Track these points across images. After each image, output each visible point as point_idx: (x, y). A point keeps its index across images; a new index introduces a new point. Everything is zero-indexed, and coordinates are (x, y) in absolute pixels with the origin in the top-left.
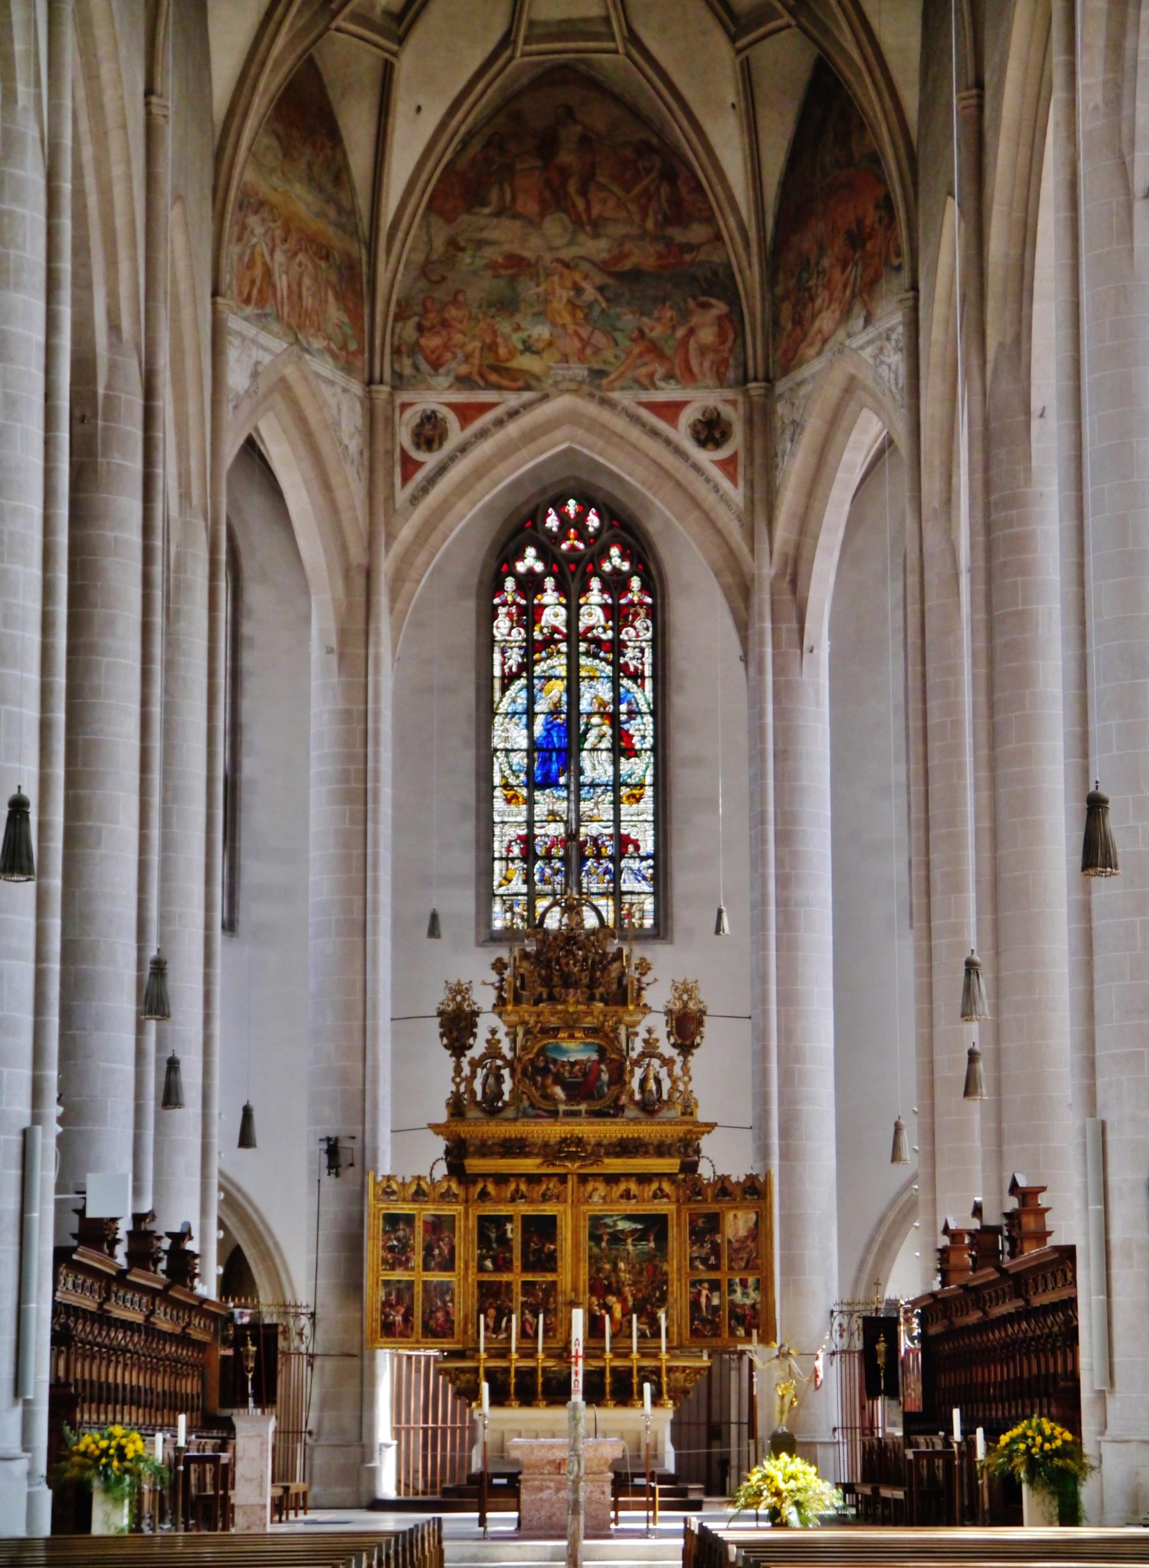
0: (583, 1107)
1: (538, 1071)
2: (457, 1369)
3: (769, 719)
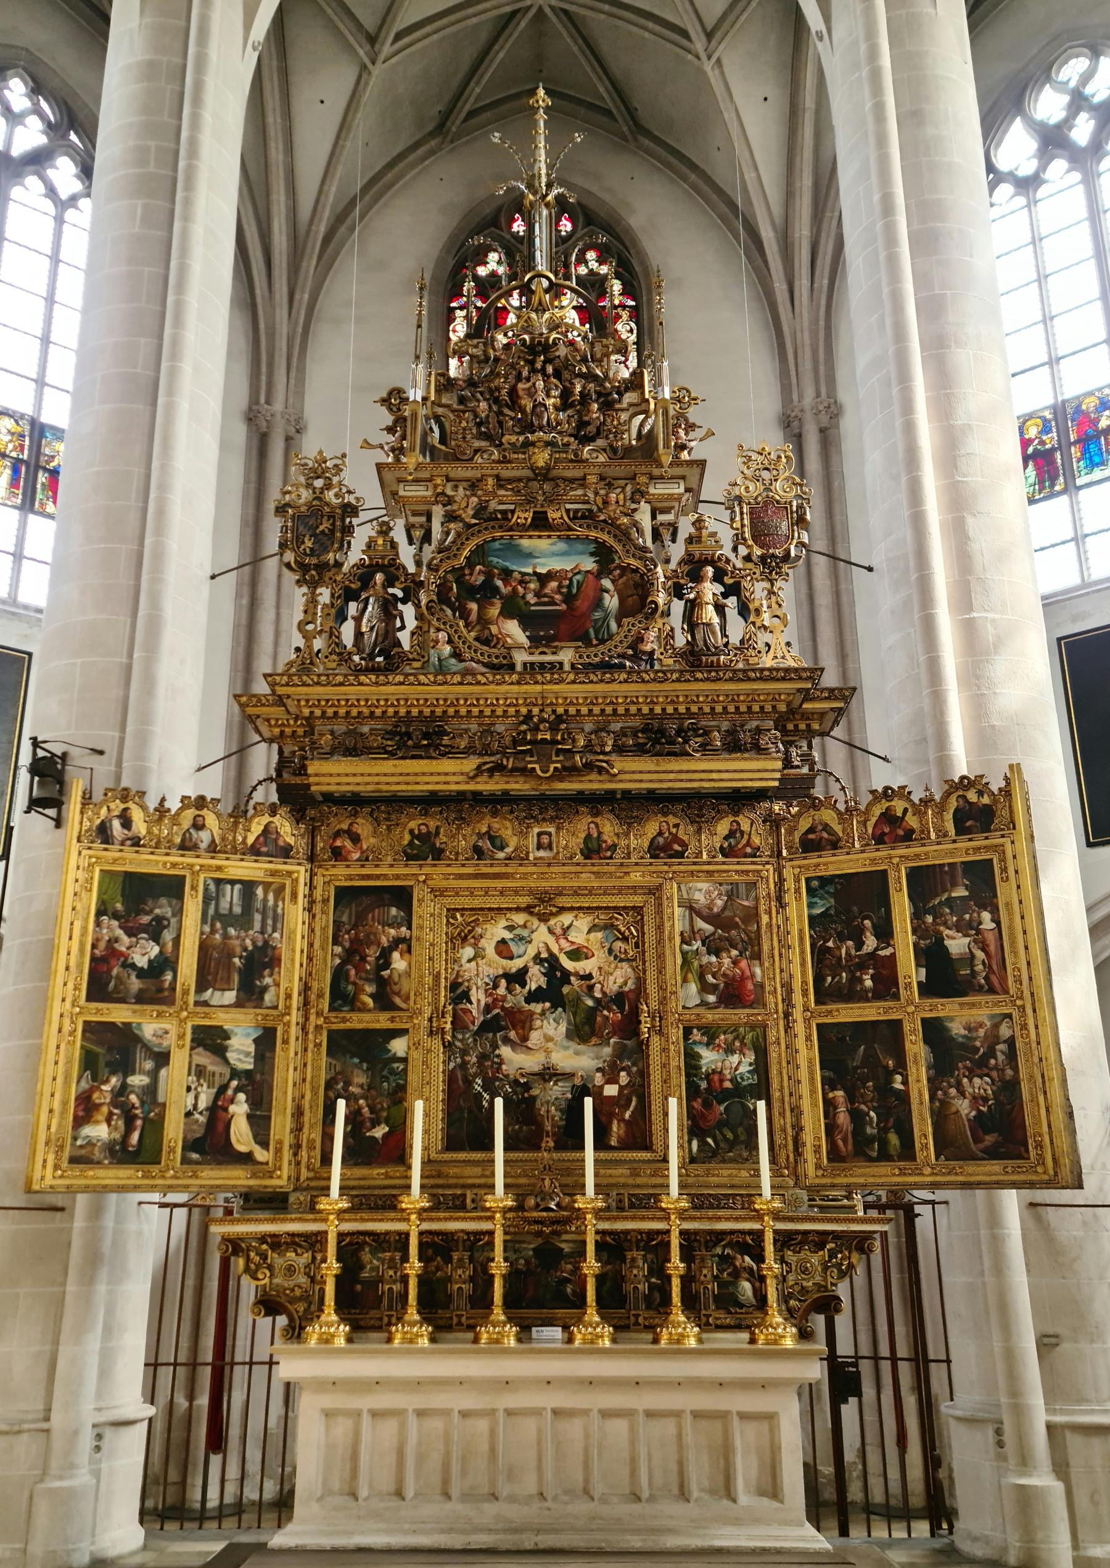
0: (566, 656)
1: (470, 592)
2: (263, 1238)
3: (886, 61)
